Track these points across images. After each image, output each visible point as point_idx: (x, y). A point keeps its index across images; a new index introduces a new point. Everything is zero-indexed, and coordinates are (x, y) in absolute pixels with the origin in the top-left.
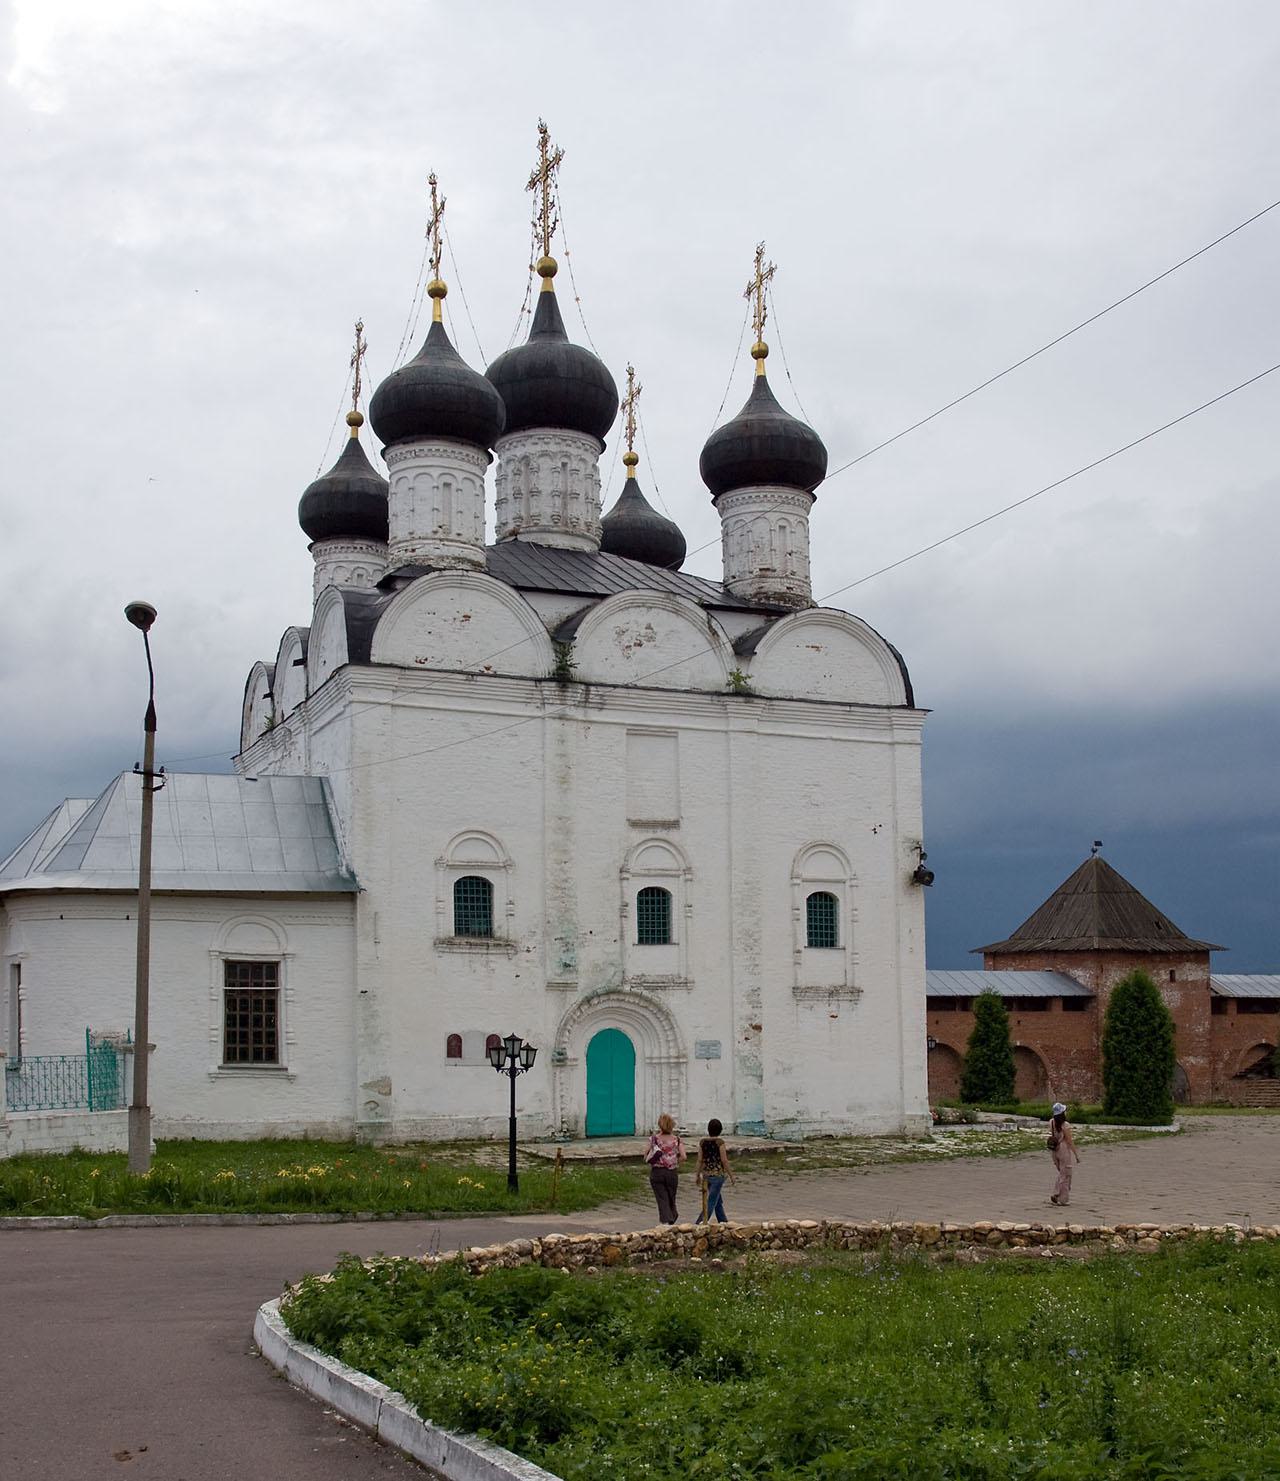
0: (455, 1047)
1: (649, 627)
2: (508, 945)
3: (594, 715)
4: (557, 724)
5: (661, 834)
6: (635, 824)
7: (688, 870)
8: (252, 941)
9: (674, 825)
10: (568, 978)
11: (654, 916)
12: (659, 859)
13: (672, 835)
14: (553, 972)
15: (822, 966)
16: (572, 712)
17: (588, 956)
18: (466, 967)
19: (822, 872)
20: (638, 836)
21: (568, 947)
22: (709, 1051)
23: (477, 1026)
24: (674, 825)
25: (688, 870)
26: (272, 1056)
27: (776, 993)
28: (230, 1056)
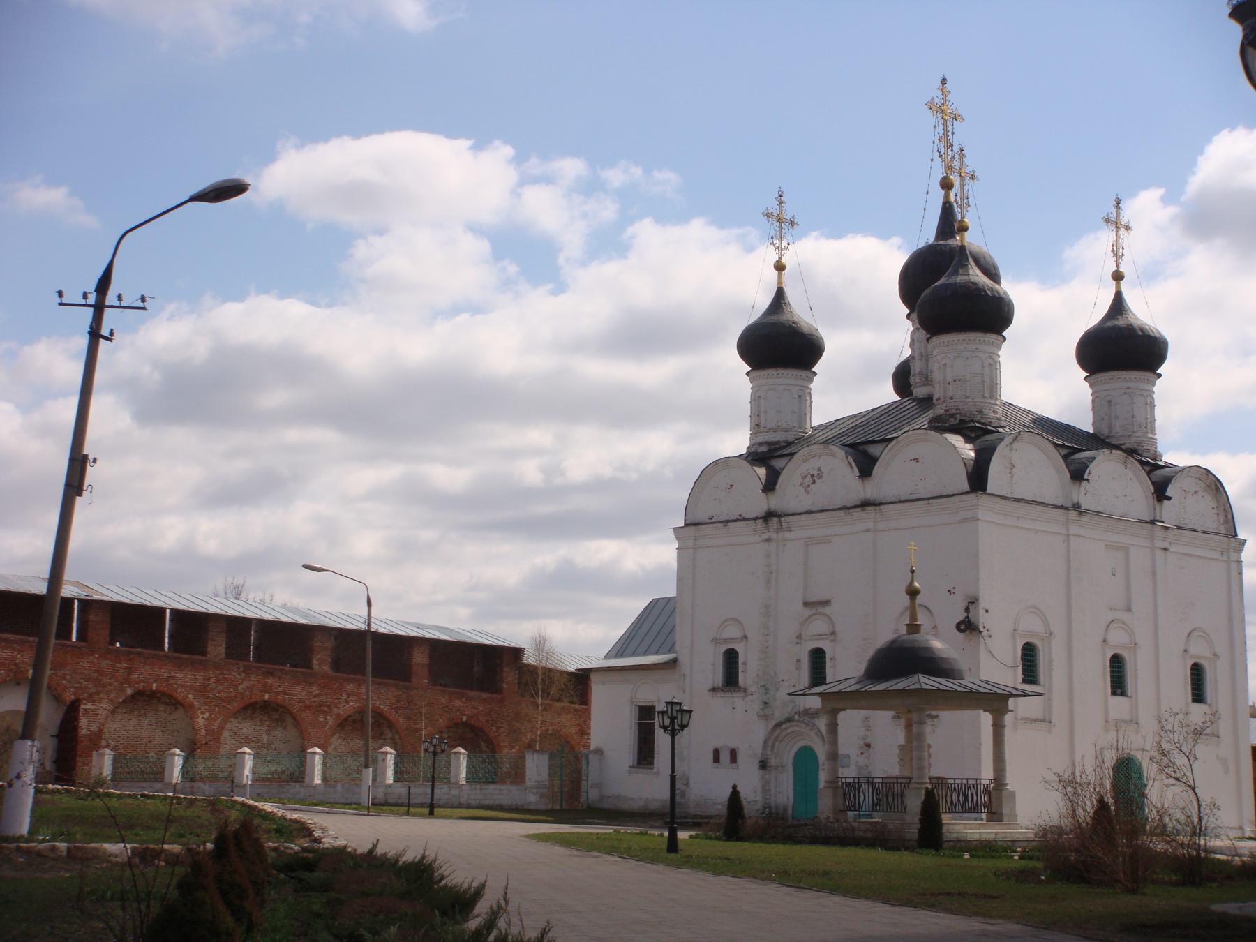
0: (716, 759)
1: (819, 469)
3: (787, 535)
4: (766, 545)
5: (821, 609)
6: (806, 604)
7: (833, 633)
9: (826, 603)
10: (768, 711)
12: (819, 626)
13: (827, 610)
14: (757, 706)
16: (774, 536)
20: (807, 612)
21: (767, 690)
23: (725, 742)
24: (826, 603)
25: (833, 633)
26: (651, 763)
28: (639, 763)
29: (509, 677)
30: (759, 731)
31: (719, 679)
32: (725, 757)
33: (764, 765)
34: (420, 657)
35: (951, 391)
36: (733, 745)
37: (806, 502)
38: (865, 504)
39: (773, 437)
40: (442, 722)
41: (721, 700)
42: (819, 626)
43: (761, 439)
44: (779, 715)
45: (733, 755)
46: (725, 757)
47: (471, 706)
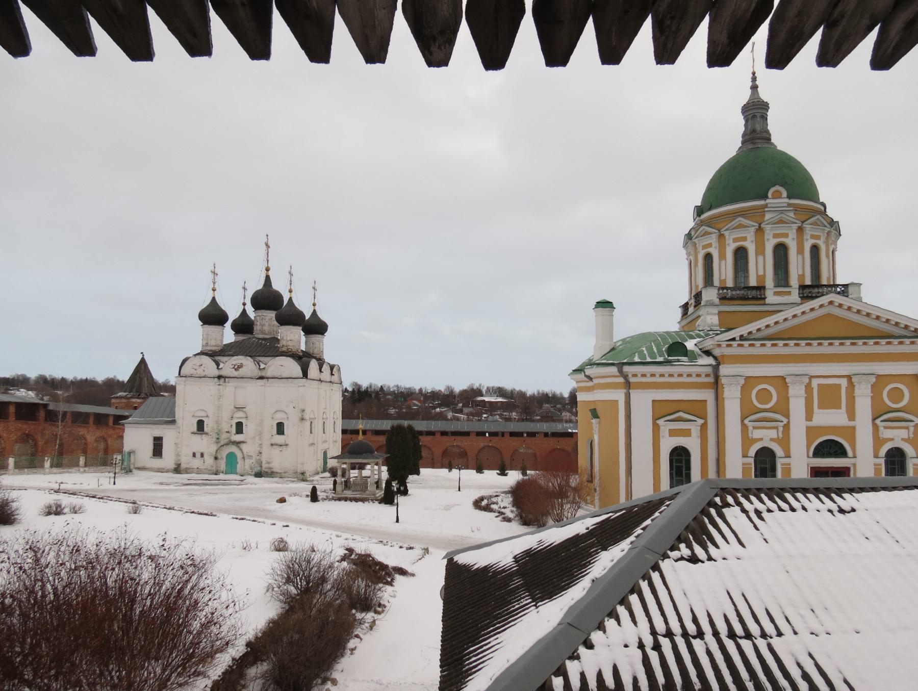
0: (194, 455)
2: (207, 434)
8: (158, 433)
11: (239, 428)
14: (214, 439)
15: (280, 439)
17: (224, 436)
18: (197, 438)
19: (280, 417)
22: (250, 457)
23: (198, 450)
27: (266, 443)
29: (42, 414)
30: (214, 447)
31: (195, 428)
32: (198, 455)
33: (216, 458)
34: (12, 409)
35: (290, 343)
36: (202, 451)
37: (236, 374)
38: (261, 378)
39: (213, 348)
40: (19, 434)
41: (198, 437)
42: (240, 414)
43: (209, 348)
44: (222, 443)
45: (202, 455)
46: (198, 455)
47: (26, 427)
